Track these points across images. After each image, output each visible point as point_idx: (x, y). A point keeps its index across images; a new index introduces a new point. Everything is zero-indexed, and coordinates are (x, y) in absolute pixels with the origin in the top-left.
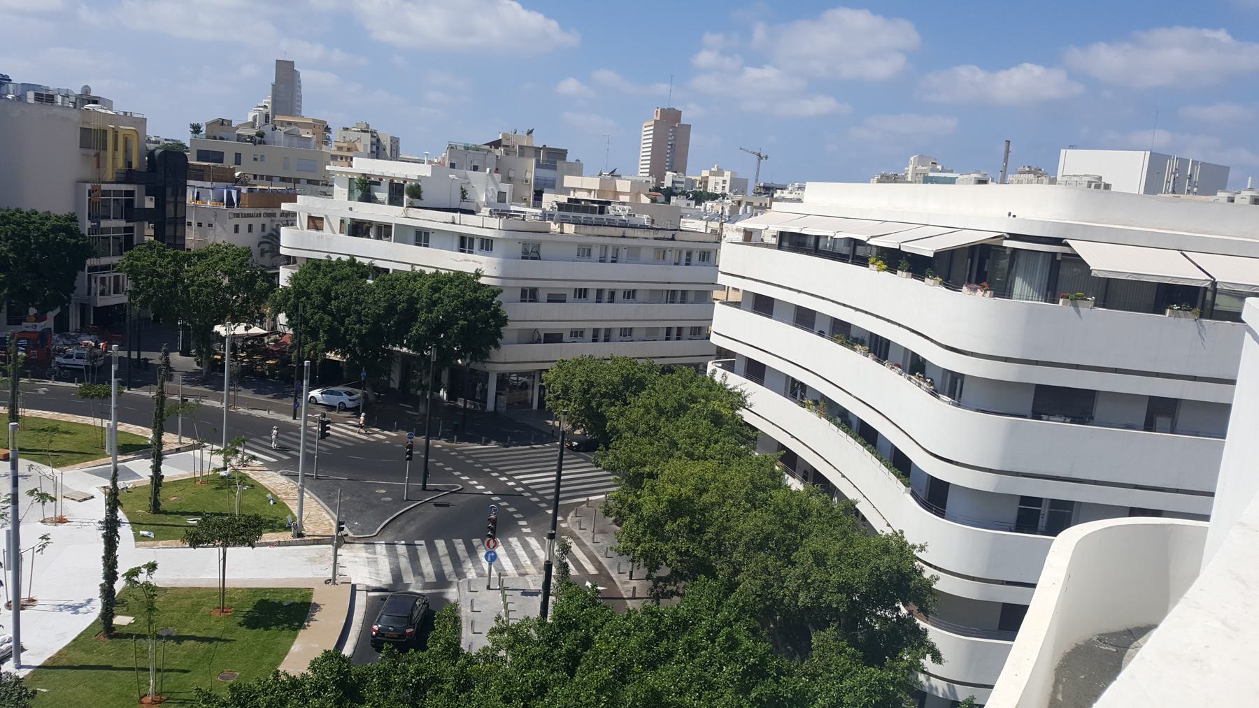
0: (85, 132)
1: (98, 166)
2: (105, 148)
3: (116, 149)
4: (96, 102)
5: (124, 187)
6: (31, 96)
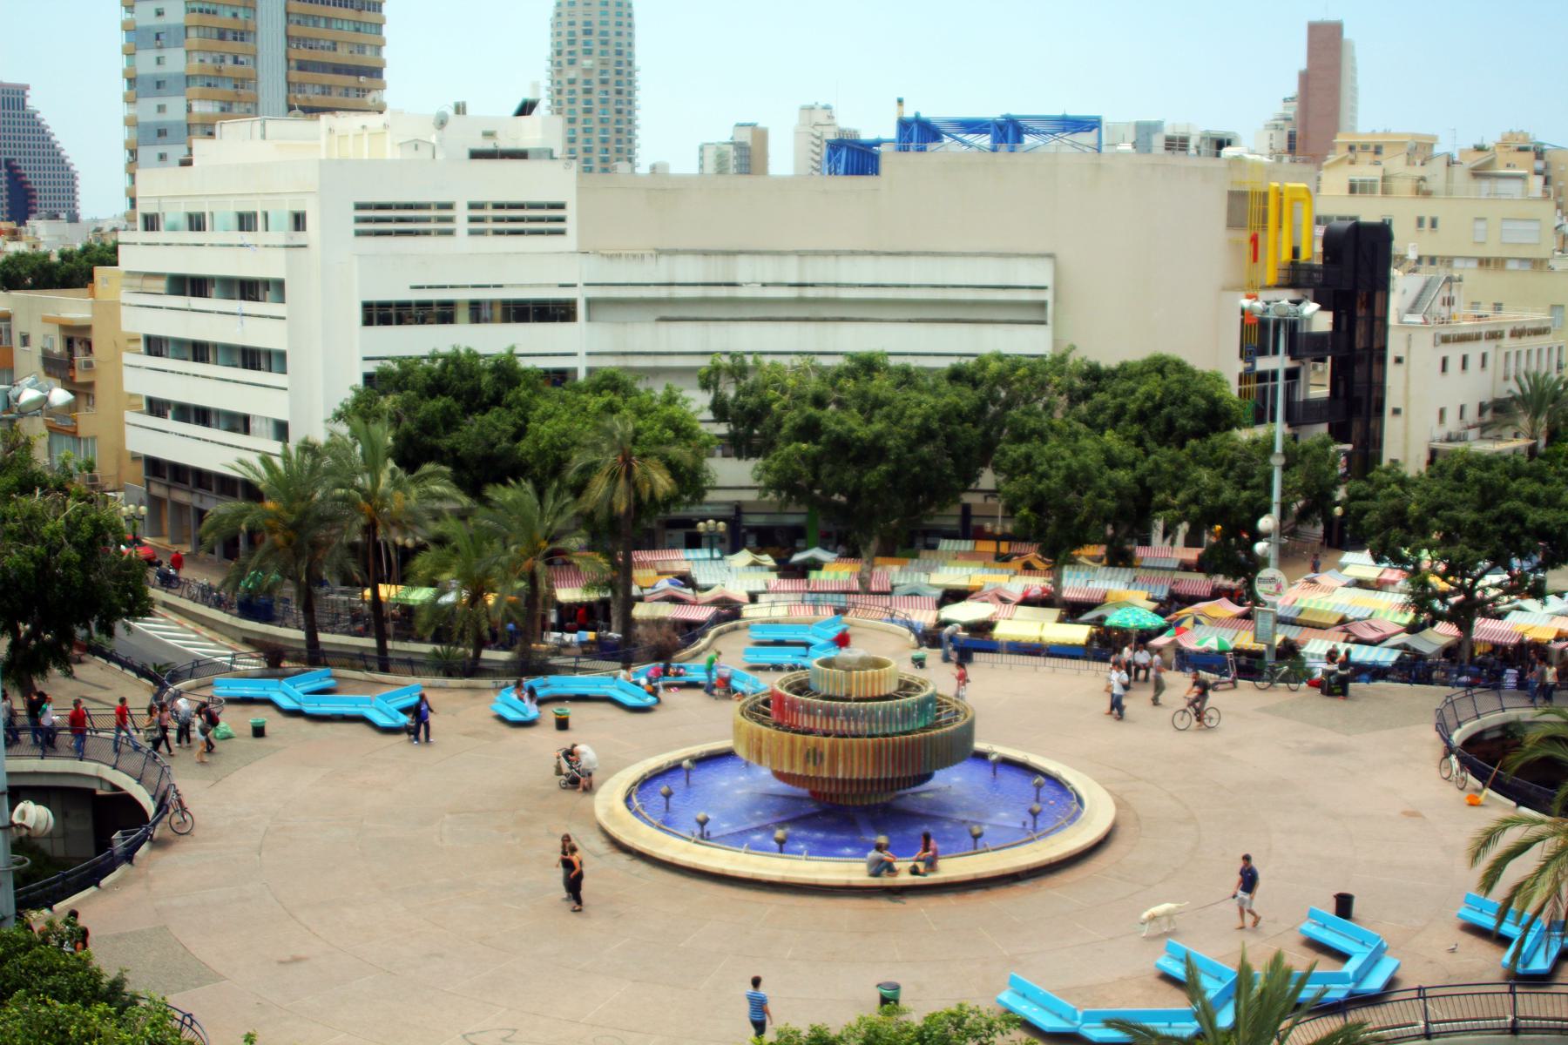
0: (1237, 199)
1: (1255, 259)
2: (1265, 228)
4: (1229, 143)
6: (1158, 142)
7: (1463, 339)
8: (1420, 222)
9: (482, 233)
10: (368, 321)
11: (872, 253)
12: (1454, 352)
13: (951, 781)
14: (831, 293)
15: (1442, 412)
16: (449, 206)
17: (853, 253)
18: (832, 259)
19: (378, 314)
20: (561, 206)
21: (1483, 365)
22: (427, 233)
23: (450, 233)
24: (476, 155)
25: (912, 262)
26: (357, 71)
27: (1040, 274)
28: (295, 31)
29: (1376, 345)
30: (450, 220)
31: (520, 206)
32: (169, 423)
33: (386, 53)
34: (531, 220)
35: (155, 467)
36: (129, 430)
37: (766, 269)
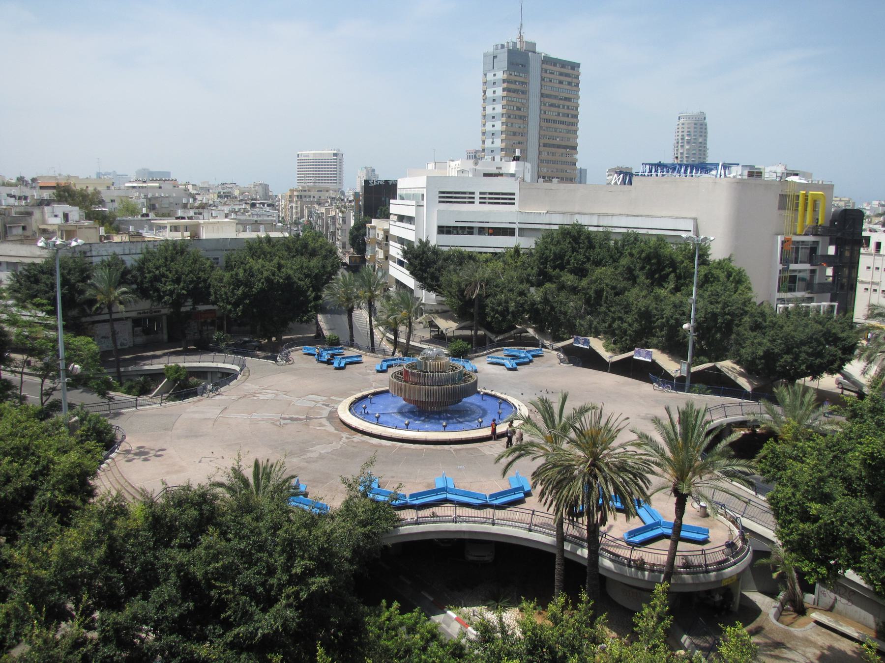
3: (805, 210)
5: (810, 238)
9: (484, 203)
13: (471, 400)
16: (473, 193)
17: (620, 215)
20: (514, 194)
22: (465, 202)
23: (473, 203)
24: (485, 175)
26: (566, 147)
28: (542, 133)
33: (578, 141)
35: (398, 282)
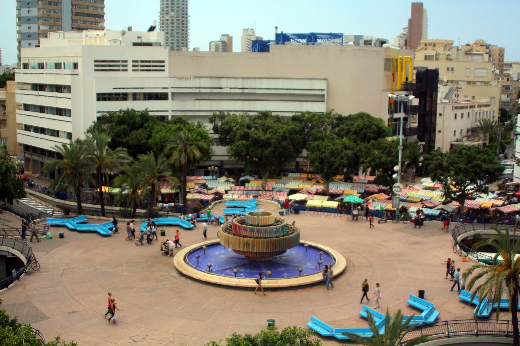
1: (394, 81)
2: (397, 71)
3: (402, 70)
4: (385, 43)
6: (362, 42)
7: (462, 108)
8: (448, 69)
10: (98, 99)
11: (267, 78)
12: (459, 112)
13: (292, 253)
14: (253, 91)
15: (455, 132)
17: (260, 78)
18: (253, 80)
19: (102, 97)
20: (163, 62)
21: (468, 116)
22: (118, 70)
23: (126, 70)
24: (135, 44)
25: (280, 81)
26: (95, 16)
27: (322, 85)
29: (433, 110)
30: (126, 66)
31: (149, 62)
32: (32, 133)
33: (105, 10)
34: (153, 66)
35: (27, 148)
36: (18, 136)
37: (231, 83)
